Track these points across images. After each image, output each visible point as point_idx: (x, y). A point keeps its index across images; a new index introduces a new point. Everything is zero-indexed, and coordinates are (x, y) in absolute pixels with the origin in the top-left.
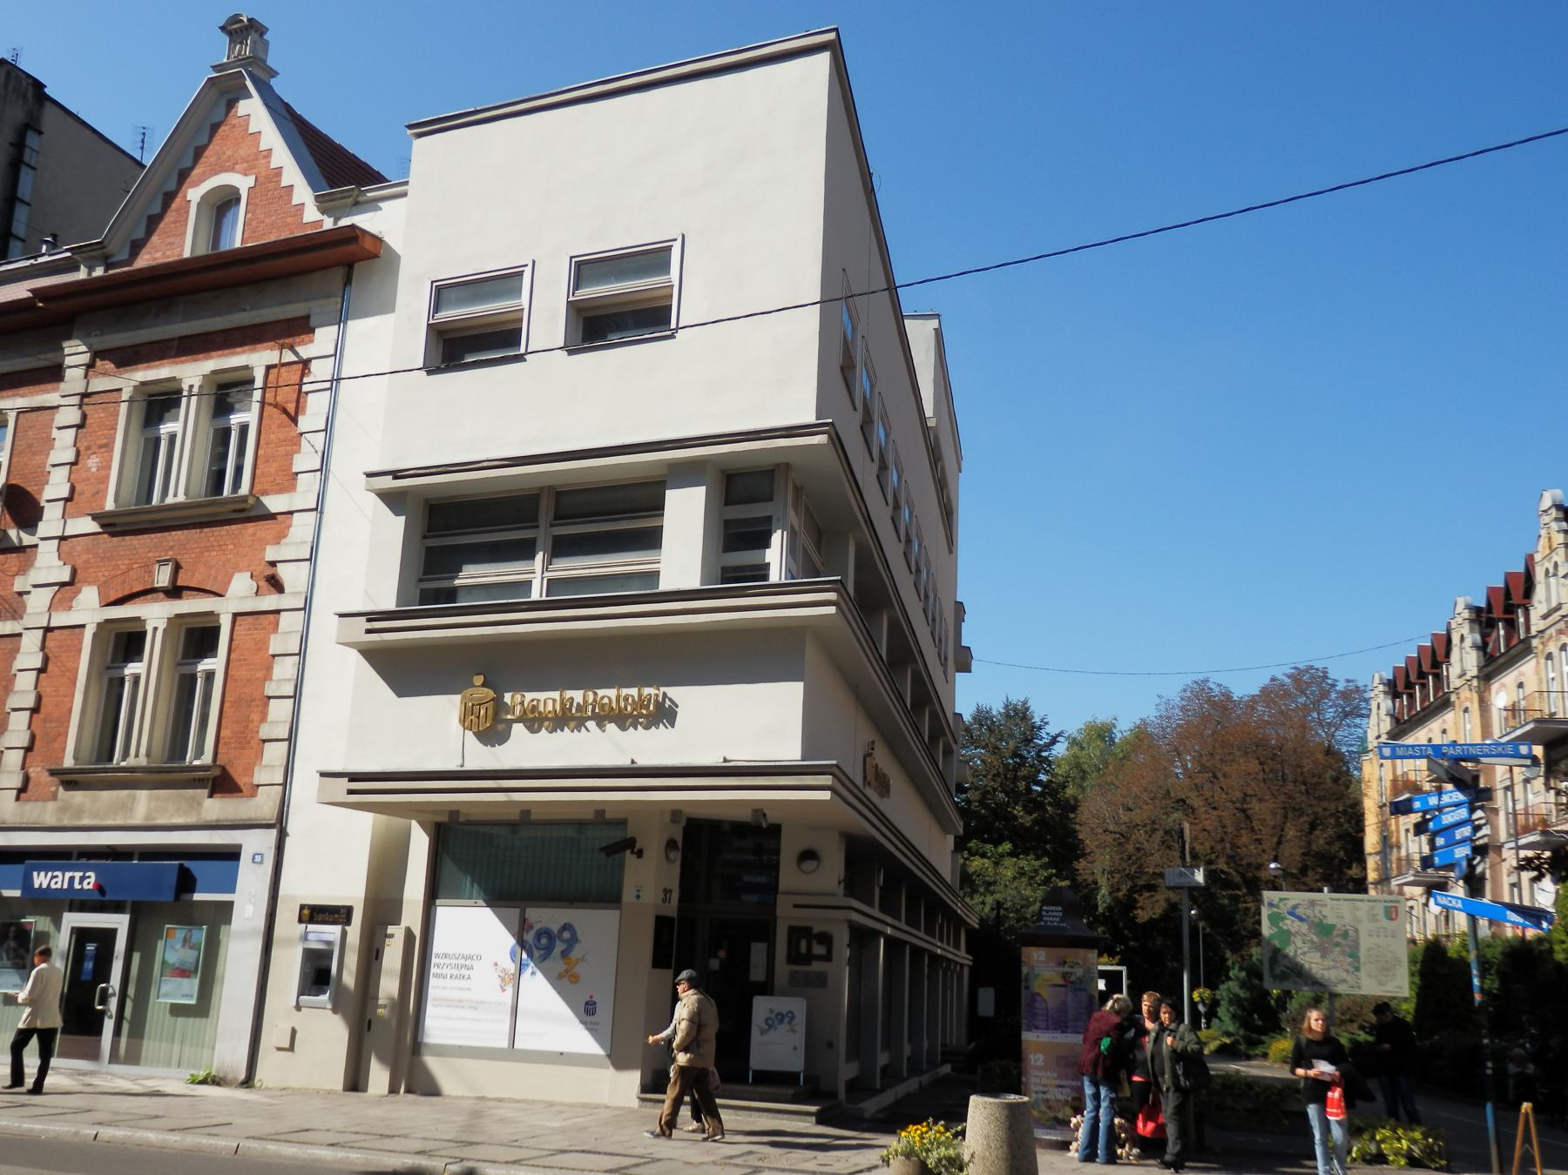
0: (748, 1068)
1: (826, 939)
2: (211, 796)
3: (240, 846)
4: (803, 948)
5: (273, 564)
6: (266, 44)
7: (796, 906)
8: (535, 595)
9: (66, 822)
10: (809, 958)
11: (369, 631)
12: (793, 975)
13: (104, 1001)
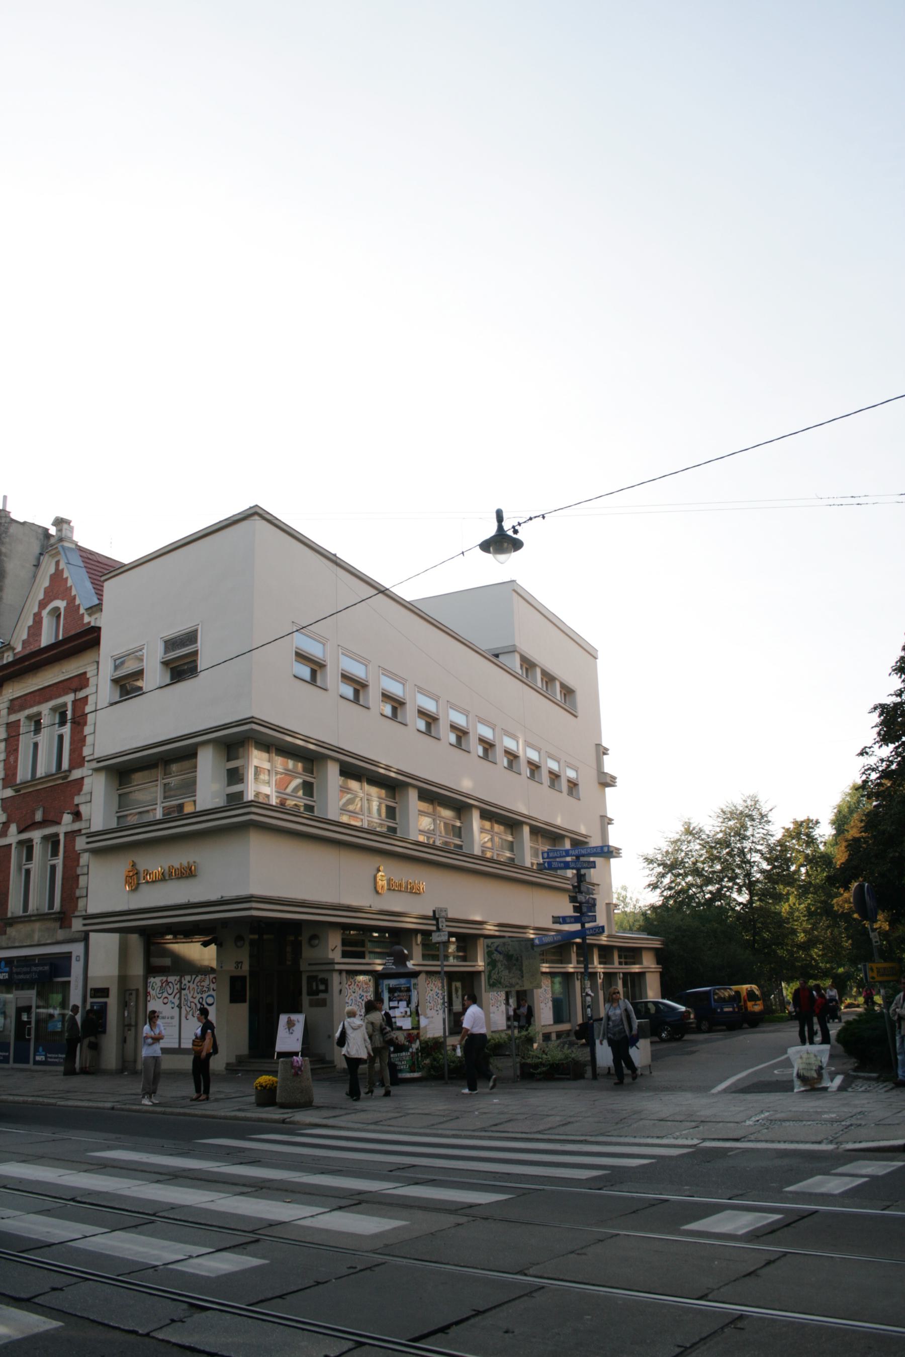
0: (274, 1051)
1: (325, 982)
2: (61, 927)
3: (71, 953)
4: (314, 988)
5: (77, 805)
6: (72, 528)
7: (310, 964)
8: (159, 815)
9: (10, 945)
10: (317, 992)
11: (88, 843)
13: (29, 1034)
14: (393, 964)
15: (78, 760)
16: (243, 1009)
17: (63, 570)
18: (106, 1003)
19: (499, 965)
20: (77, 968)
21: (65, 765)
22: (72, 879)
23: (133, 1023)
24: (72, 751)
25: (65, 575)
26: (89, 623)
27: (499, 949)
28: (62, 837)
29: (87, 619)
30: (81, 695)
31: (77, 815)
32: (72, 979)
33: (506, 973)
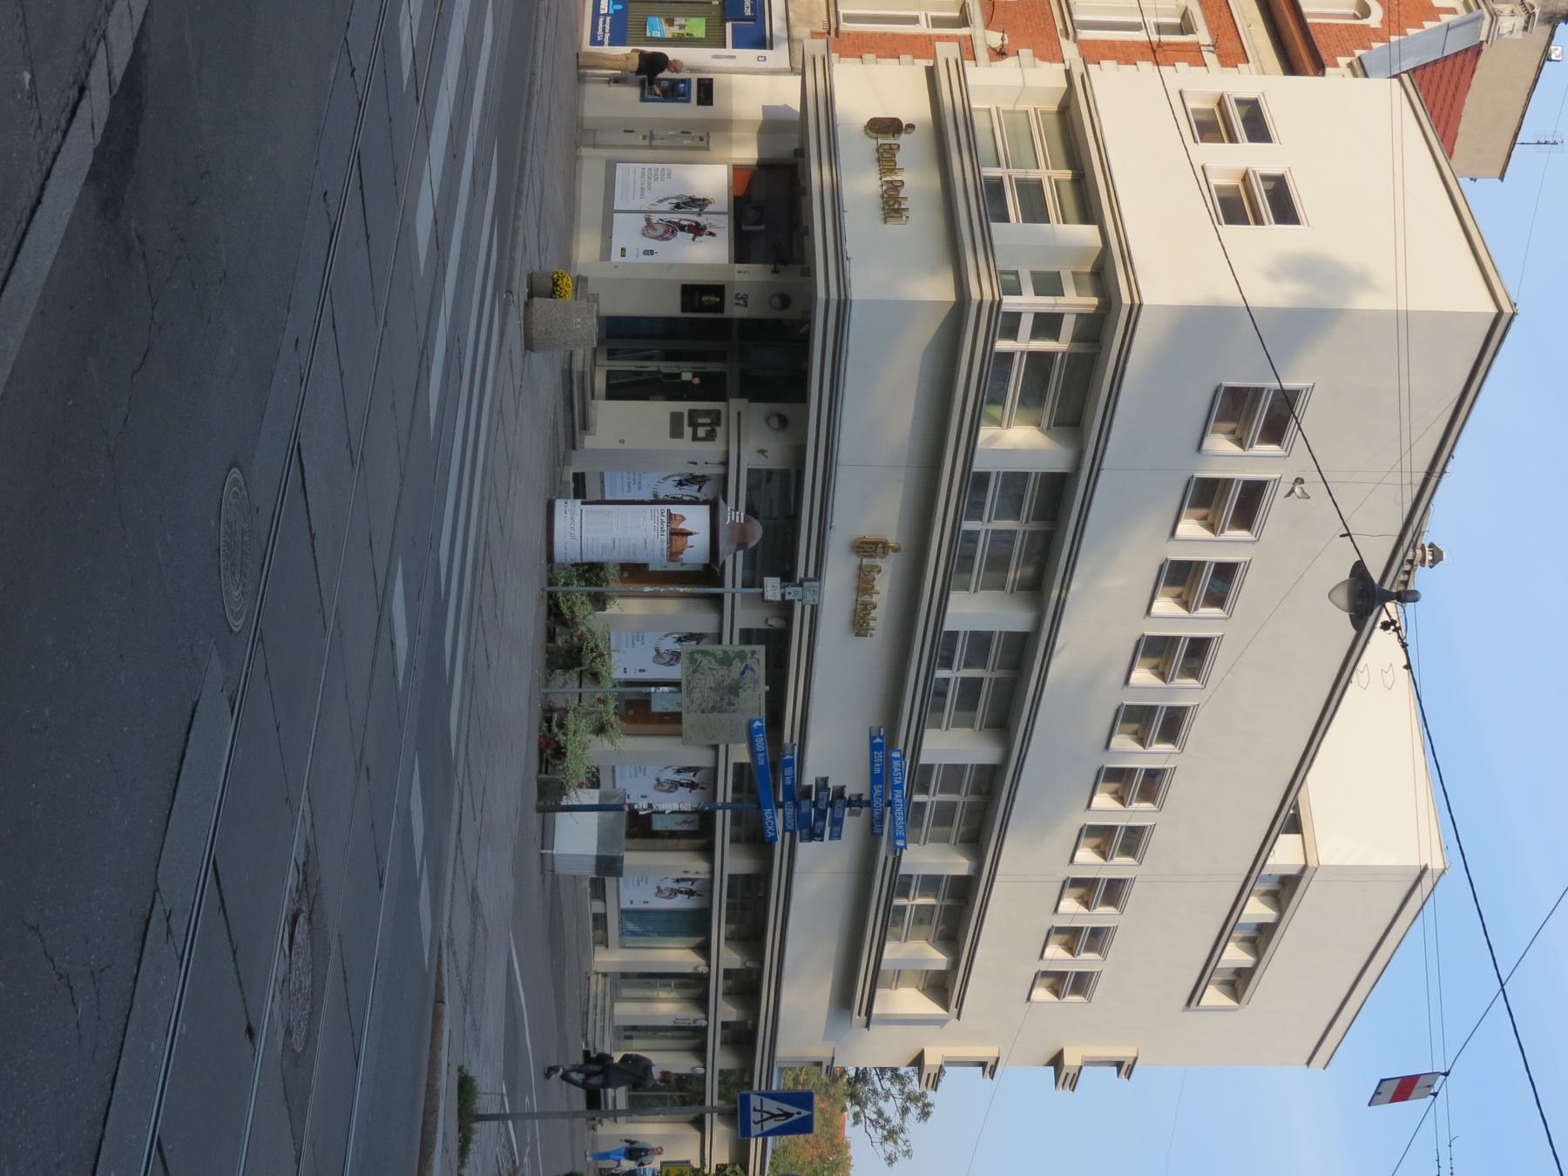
1: (711, 436)
4: (700, 421)
10: (694, 425)
12: (680, 415)
14: (733, 522)
15: (1093, 53)
16: (671, 307)
17: (1439, 20)
18: (688, 101)
19: (724, 671)
20: (748, 56)
21: (1085, 35)
22: (889, 47)
23: (655, 143)
24: (1111, 45)
25: (1428, 25)
26: (1336, 65)
27: (748, 672)
28: (964, 31)
29: (1343, 61)
30: (1210, 58)
31: (1000, 53)
32: (729, 51)
33: (711, 682)
